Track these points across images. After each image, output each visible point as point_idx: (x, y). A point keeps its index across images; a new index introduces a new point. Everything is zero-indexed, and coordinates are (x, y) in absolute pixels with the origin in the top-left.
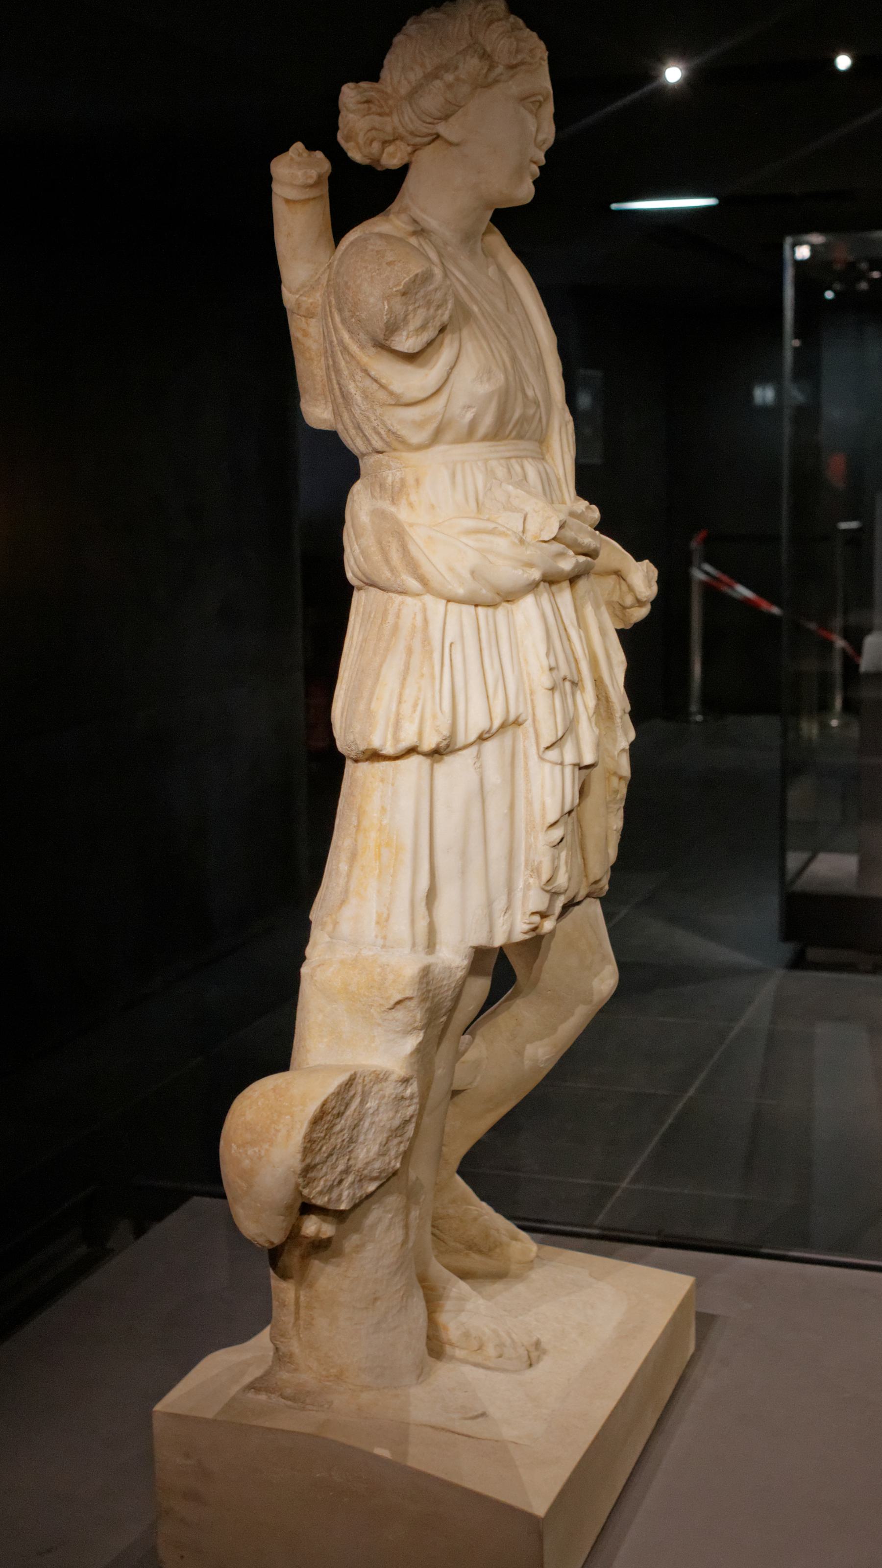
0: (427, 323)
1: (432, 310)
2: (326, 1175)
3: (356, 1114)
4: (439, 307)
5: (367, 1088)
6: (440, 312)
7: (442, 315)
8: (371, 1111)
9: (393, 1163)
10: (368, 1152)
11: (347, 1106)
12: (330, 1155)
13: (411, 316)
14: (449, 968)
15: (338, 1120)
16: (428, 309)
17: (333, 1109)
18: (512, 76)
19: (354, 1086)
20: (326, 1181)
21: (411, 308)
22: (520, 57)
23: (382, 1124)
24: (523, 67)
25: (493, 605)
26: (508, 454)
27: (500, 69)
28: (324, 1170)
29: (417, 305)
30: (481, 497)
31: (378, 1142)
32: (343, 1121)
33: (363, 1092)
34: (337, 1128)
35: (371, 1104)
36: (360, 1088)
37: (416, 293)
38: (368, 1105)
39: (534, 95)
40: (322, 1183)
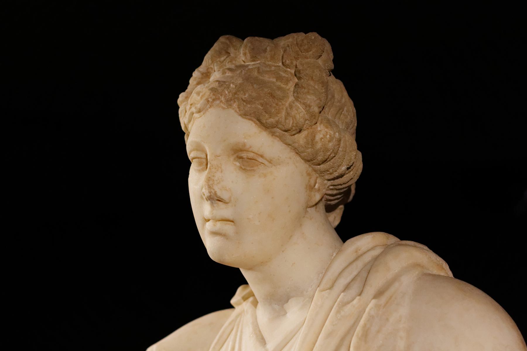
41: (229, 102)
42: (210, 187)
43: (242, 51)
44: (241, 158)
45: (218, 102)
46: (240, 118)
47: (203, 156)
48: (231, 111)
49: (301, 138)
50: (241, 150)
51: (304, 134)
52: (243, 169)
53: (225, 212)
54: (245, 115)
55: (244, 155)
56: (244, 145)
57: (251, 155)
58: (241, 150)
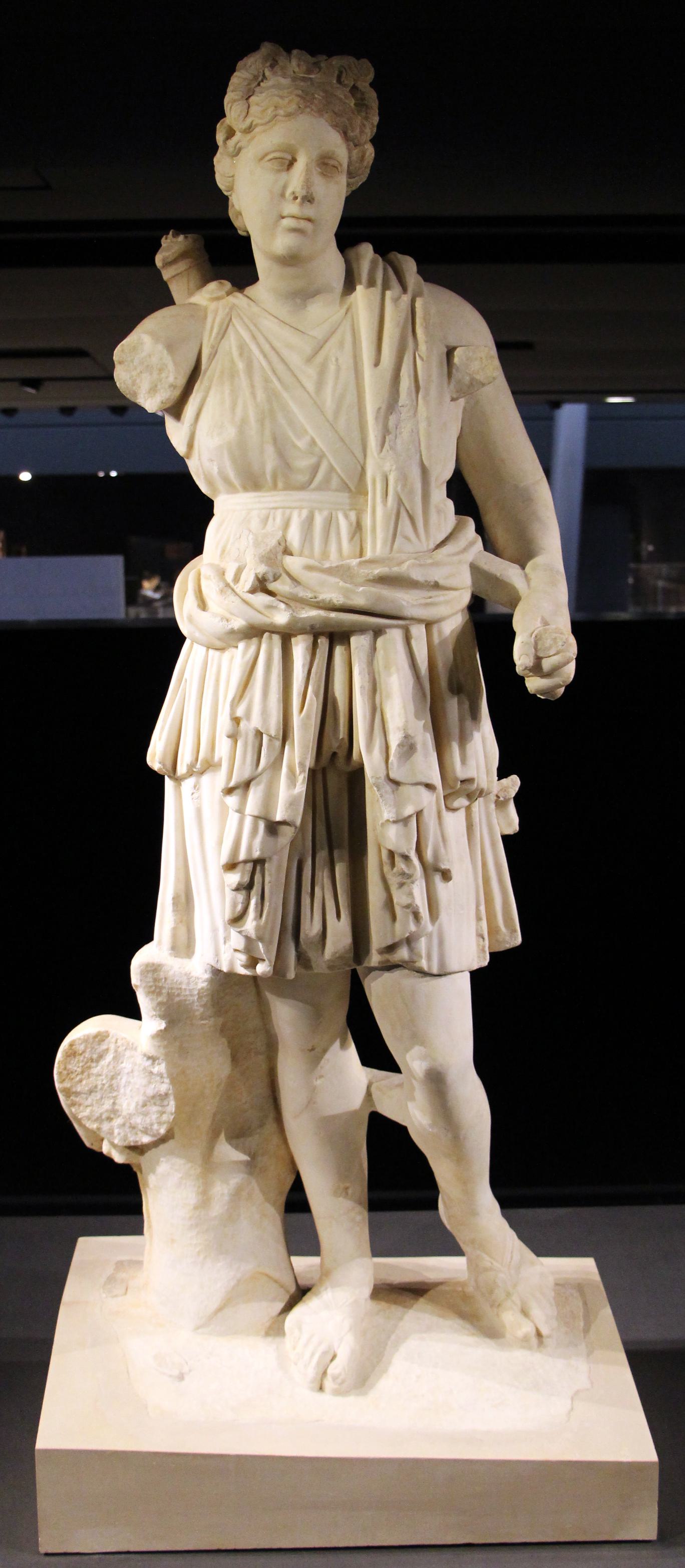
0: (156, 386)
1: (155, 375)
2: (92, 1105)
3: (111, 1067)
4: (161, 370)
5: (120, 1049)
6: (163, 375)
7: (167, 377)
8: (126, 1071)
9: (155, 1127)
10: (129, 1104)
11: (101, 1057)
12: (91, 1092)
13: (138, 381)
14: (186, 974)
15: (94, 1065)
16: (151, 374)
17: (84, 1052)
18: (250, 141)
19: (106, 1042)
20: (92, 1111)
21: (134, 373)
22: (248, 121)
23: (137, 1086)
24: (257, 130)
25: (222, 649)
26: (272, 505)
27: (238, 136)
28: (89, 1101)
29: (138, 371)
30: (229, 547)
31: (136, 1099)
32: (99, 1068)
33: (116, 1051)
34: (95, 1071)
35: (126, 1066)
36: (112, 1047)
37: (132, 361)
38: (123, 1065)
39: (266, 155)
40: (88, 1110)
41: (320, 112)
42: (308, 187)
43: (294, 62)
44: (326, 164)
45: (308, 110)
46: (330, 128)
47: (290, 158)
48: (322, 121)
49: (355, 152)
50: (330, 158)
51: (358, 149)
52: (323, 174)
53: (309, 211)
54: (335, 126)
55: (332, 162)
56: (334, 153)
57: (336, 163)
58: (330, 158)
